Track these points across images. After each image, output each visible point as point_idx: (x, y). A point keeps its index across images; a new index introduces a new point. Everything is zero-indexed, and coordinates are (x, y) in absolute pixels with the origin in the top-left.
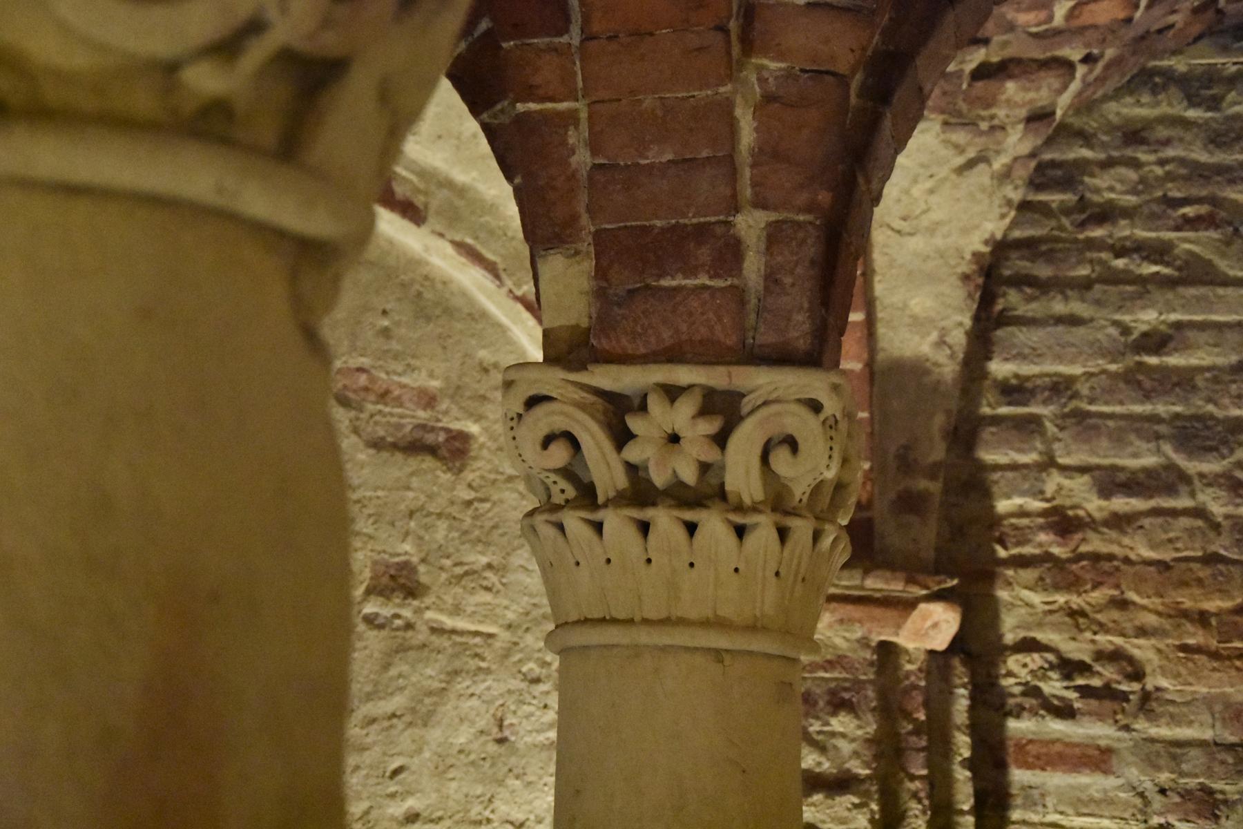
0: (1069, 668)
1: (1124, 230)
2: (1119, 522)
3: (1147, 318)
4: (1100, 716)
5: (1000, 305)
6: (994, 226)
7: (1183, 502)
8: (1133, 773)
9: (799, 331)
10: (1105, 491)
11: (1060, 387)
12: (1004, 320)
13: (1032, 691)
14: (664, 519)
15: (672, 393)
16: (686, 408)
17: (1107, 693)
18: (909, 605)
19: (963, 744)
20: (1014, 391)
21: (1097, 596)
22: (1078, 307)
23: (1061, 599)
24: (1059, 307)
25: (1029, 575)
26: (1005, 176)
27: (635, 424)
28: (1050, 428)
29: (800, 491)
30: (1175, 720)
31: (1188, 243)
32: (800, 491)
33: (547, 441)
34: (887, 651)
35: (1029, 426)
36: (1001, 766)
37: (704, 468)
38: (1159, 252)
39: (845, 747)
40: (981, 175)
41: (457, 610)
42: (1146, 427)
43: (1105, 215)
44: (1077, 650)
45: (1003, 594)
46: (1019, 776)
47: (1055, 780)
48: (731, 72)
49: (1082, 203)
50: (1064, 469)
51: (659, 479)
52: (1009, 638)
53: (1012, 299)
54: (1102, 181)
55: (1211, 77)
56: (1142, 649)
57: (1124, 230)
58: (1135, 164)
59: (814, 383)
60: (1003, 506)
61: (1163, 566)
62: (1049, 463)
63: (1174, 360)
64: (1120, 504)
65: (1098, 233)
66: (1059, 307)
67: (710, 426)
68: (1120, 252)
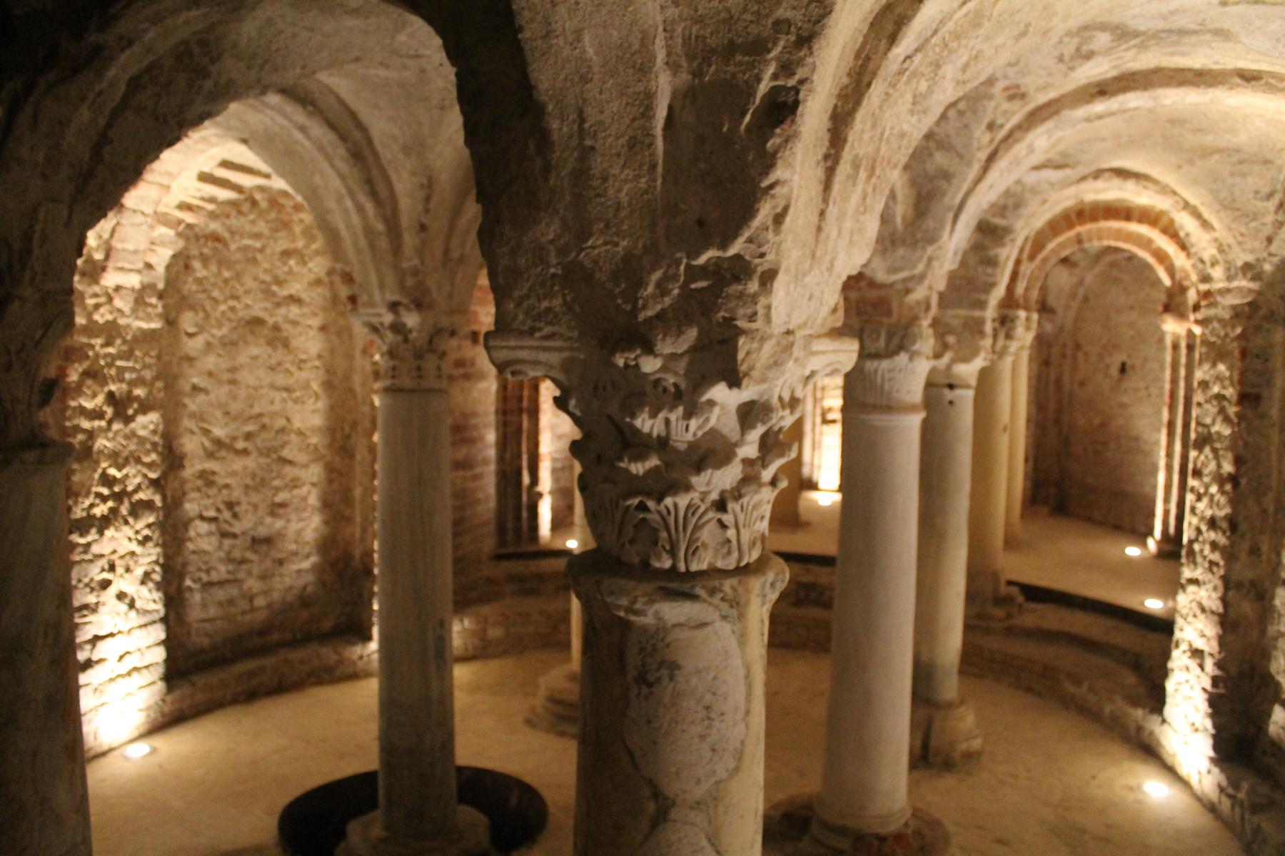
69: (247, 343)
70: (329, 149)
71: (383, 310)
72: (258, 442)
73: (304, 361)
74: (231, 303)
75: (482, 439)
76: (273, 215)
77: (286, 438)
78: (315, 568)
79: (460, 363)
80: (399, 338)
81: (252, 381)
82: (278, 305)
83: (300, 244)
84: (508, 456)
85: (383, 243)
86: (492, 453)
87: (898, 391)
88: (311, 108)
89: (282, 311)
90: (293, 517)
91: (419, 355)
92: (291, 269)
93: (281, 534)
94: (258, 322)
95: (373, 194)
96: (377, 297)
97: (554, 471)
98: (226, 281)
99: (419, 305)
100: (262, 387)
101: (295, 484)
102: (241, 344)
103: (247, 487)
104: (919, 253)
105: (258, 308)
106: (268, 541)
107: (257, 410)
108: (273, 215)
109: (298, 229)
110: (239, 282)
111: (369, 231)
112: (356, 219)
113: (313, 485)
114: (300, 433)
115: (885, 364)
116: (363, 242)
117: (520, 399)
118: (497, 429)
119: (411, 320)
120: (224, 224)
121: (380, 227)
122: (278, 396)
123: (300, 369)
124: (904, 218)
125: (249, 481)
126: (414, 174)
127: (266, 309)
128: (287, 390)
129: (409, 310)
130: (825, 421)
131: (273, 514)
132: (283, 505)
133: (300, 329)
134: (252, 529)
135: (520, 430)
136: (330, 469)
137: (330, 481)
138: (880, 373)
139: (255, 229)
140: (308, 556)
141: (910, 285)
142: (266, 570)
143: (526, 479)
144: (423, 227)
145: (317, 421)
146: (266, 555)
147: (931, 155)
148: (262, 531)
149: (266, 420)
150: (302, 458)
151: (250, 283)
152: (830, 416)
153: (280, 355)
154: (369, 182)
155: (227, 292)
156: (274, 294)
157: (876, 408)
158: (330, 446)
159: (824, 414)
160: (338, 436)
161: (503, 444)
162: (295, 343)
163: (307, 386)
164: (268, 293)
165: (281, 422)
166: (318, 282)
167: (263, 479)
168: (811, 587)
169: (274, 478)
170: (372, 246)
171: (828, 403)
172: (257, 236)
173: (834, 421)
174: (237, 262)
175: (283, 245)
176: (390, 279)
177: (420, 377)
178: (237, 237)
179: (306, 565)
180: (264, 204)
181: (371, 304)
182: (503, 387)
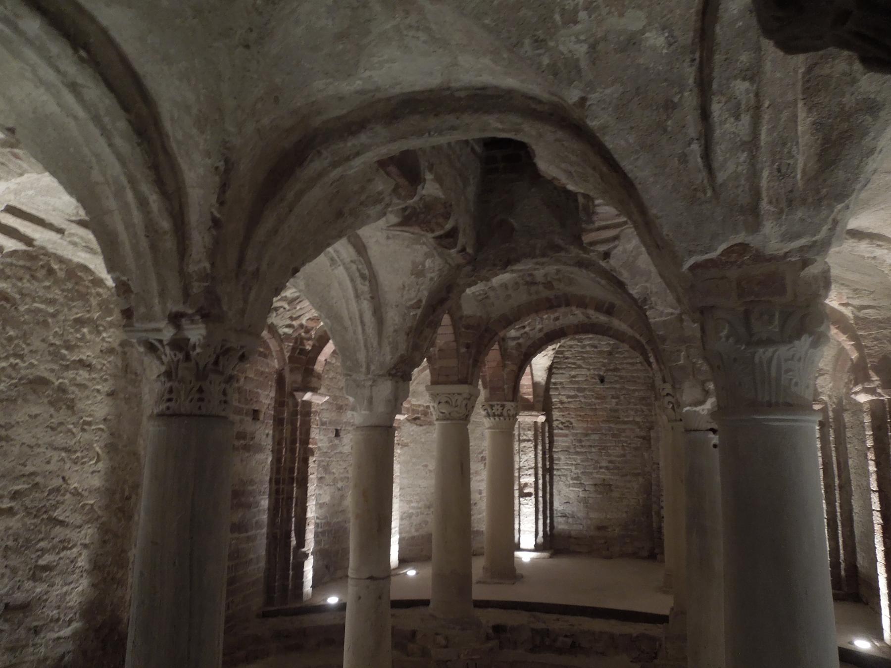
0: (562, 423)
1: (570, 360)
2: (569, 402)
3: (573, 373)
4: (566, 429)
5: (553, 371)
6: (549, 363)
7: (578, 399)
8: (571, 437)
9: (511, 399)
10: (567, 398)
11: (561, 383)
12: (553, 373)
13: (557, 427)
14: (497, 418)
15: (498, 405)
16: (499, 406)
17: (567, 426)
18: (538, 416)
19: (547, 435)
20: (555, 384)
21: (566, 413)
22: (564, 372)
23: (561, 413)
24: (561, 372)
25: (557, 410)
26: (549, 357)
27: (494, 408)
28: (560, 389)
29: (511, 415)
30: (577, 430)
31: (579, 362)
32: (511, 415)
33: (485, 410)
34: (536, 422)
35: (557, 389)
36: (553, 437)
37: (501, 413)
38: (574, 364)
39: (530, 436)
40: (546, 357)
41: (476, 418)
42: (573, 389)
43: (567, 358)
44: (563, 421)
45: (553, 413)
46: (555, 438)
47: (561, 439)
48: (503, 370)
49: (564, 357)
50: (562, 395)
51: (496, 413)
52: (554, 419)
53: (554, 371)
54: (566, 353)
55: (581, 339)
56: (572, 420)
57: (570, 360)
58: (571, 351)
59: (512, 404)
60: (553, 400)
61: (575, 408)
62: (559, 394)
63: (576, 379)
64: (570, 400)
65: (566, 361)
66: (561, 372)
67: (502, 408)
68: (569, 364)
69: (26, 401)
70: (106, 120)
71: (163, 324)
72: (27, 501)
73: (89, 424)
74: (12, 360)
75: (257, 504)
76: (69, 285)
77: (60, 498)
78: (75, 635)
79: (241, 436)
80: (180, 356)
81: (27, 438)
82: (67, 368)
83: (96, 315)
84: (278, 520)
85: (169, 244)
86: (265, 517)
87: (796, 384)
88: (83, 53)
89: (71, 374)
90: (58, 580)
91: (201, 375)
92: (84, 335)
93: (41, 600)
94: (43, 382)
95: (159, 183)
96: (157, 308)
97: (316, 535)
98: (10, 339)
99: (206, 316)
100: (39, 446)
101: (65, 545)
102: (20, 401)
103: (7, 548)
104: (825, 213)
105: (43, 370)
106: (25, 607)
107: (30, 469)
108: (69, 285)
109: (94, 302)
110: (25, 342)
111: (151, 228)
112: (137, 217)
113: (85, 546)
114: (76, 493)
115: (783, 351)
116: (144, 243)
117: (292, 470)
118: (270, 495)
119: (196, 333)
120: (14, 285)
121: (165, 224)
122: (55, 456)
123: (83, 430)
124: (804, 172)
125: (10, 543)
126: (208, 154)
127: (52, 371)
128: (67, 450)
129: (193, 322)
130: (523, 495)
131: (34, 578)
132: (47, 568)
133: (87, 393)
134: (7, 594)
135: (290, 498)
136: (104, 529)
137: (105, 542)
138: (775, 362)
139: (50, 296)
140: (70, 622)
141: (807, 256)
142: (18, 640)
143: (294, 542)
144: (216, 223)
145: (96, 482)
146: (20, 624)
147: (854, 81)
148: (19, 597)
149: (38, 479)
150: (77, 519)
151: (37, 344)
152: (526, 491)
153: (62, 415)
154: (155, 167)
155: (10, 350)
156: (63, 358)
157: (771, 406)
158: (107, 507)
159: (521, 489)
160: (118, 496)
161: (274, 510)
162: (80, 405)
163: (89, 447)
164: (55, 355)
165: (57, 482)
166: (111, 351)
167: (27, 540)
168: (546, 633)
169: (42, 540)
170: (154, 247)
171: (523, 480)
172: (51, 302)
173: (529, 495)
174: (25, 322)
175: (78, 313)
176: (174, 285)
177: (201, 400)
178: (28, 300)
179: (66, 632)
180: (61, 274)
181: (149, 317)
182: (277, 460)
